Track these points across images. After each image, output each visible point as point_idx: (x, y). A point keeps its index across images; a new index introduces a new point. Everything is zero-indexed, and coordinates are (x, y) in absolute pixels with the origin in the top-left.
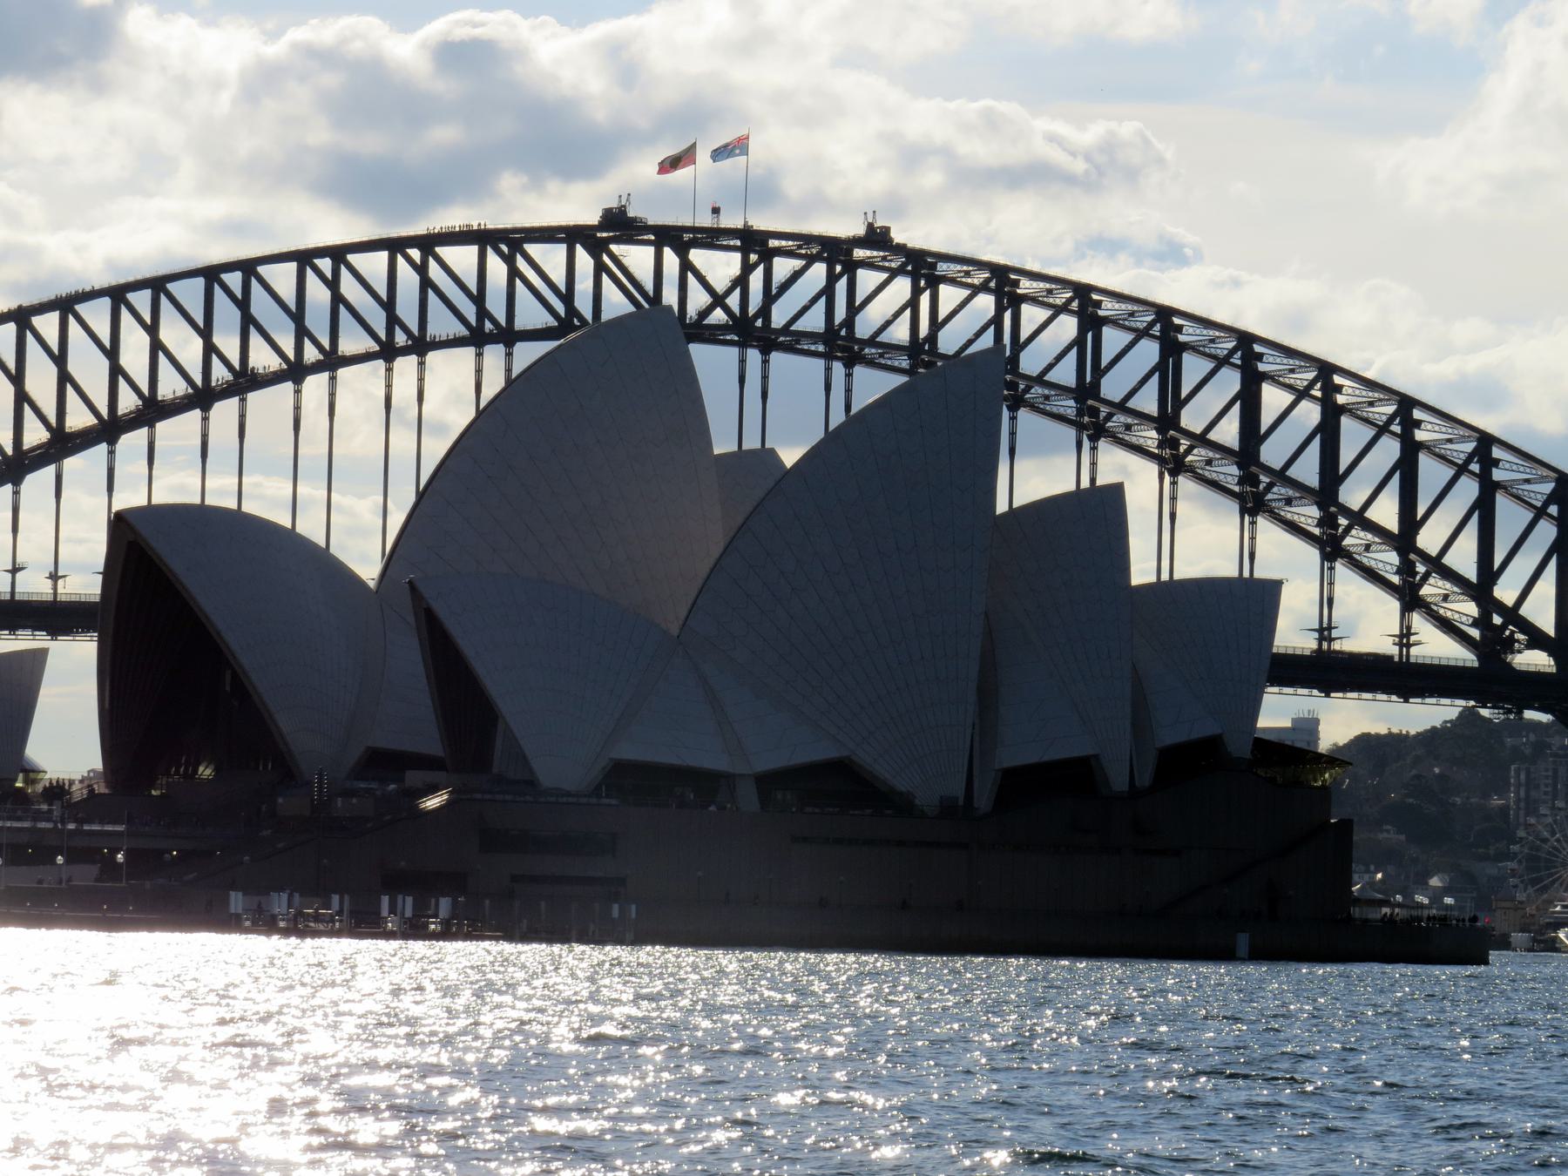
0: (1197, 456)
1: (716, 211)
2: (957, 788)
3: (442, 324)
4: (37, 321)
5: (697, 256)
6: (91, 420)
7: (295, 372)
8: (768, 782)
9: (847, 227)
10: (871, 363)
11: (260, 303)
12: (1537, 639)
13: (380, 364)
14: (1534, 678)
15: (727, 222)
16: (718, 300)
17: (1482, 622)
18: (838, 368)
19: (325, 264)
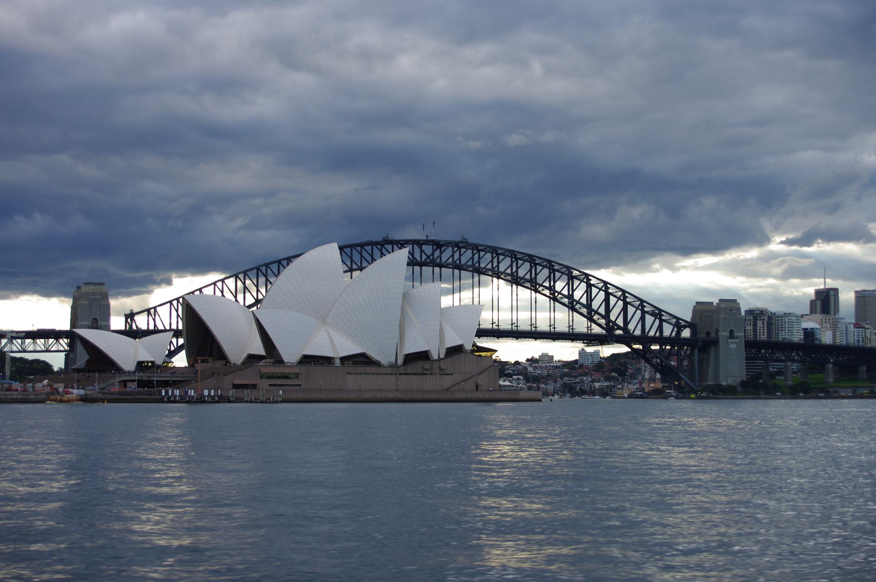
0: (541, 288)
5: (424, 247)
8: (343, 359)
9: (458, 239)
10: (465, 270)
12: (619, 328)
14: (619, 336)
16: (428, 257)
17: (607, 324)
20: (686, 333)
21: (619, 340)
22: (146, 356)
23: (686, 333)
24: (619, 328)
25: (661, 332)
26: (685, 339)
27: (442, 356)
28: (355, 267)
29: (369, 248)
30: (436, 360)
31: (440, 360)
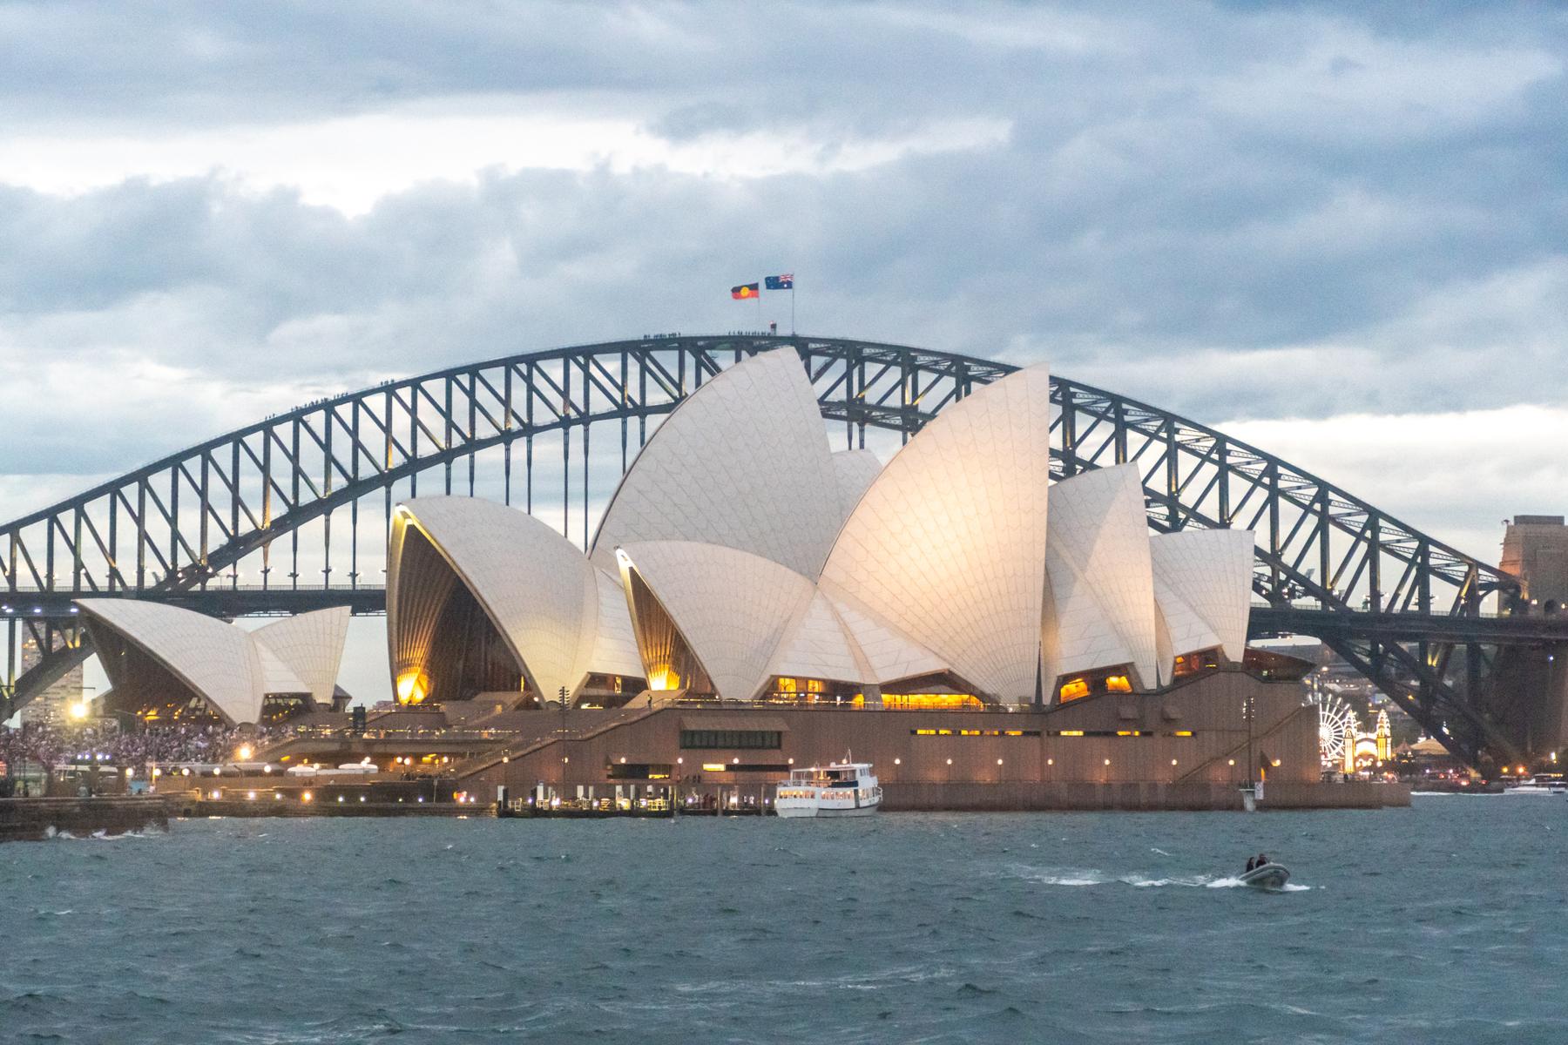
1: (774, 326)
2: (1031, 691)
3: (600, 403)
4: (338, 409)
6: (375, 472)
7: (506, 437)
11: (482, 394)
13: (561, 431)
15: (781, 332)
18: (855, 426)
19: (523, 367)
20: (1490, 605)
21: (1303, 621)
22: (285, 682)
23: (1490, 605)
24: (1310, 589)
25: (1425, 599)
26: (1489, 623)
27: (1166, 681)
28: (573, 414)
29: (668, 359)
30: (1149, 693)
31: (1161, 691)
